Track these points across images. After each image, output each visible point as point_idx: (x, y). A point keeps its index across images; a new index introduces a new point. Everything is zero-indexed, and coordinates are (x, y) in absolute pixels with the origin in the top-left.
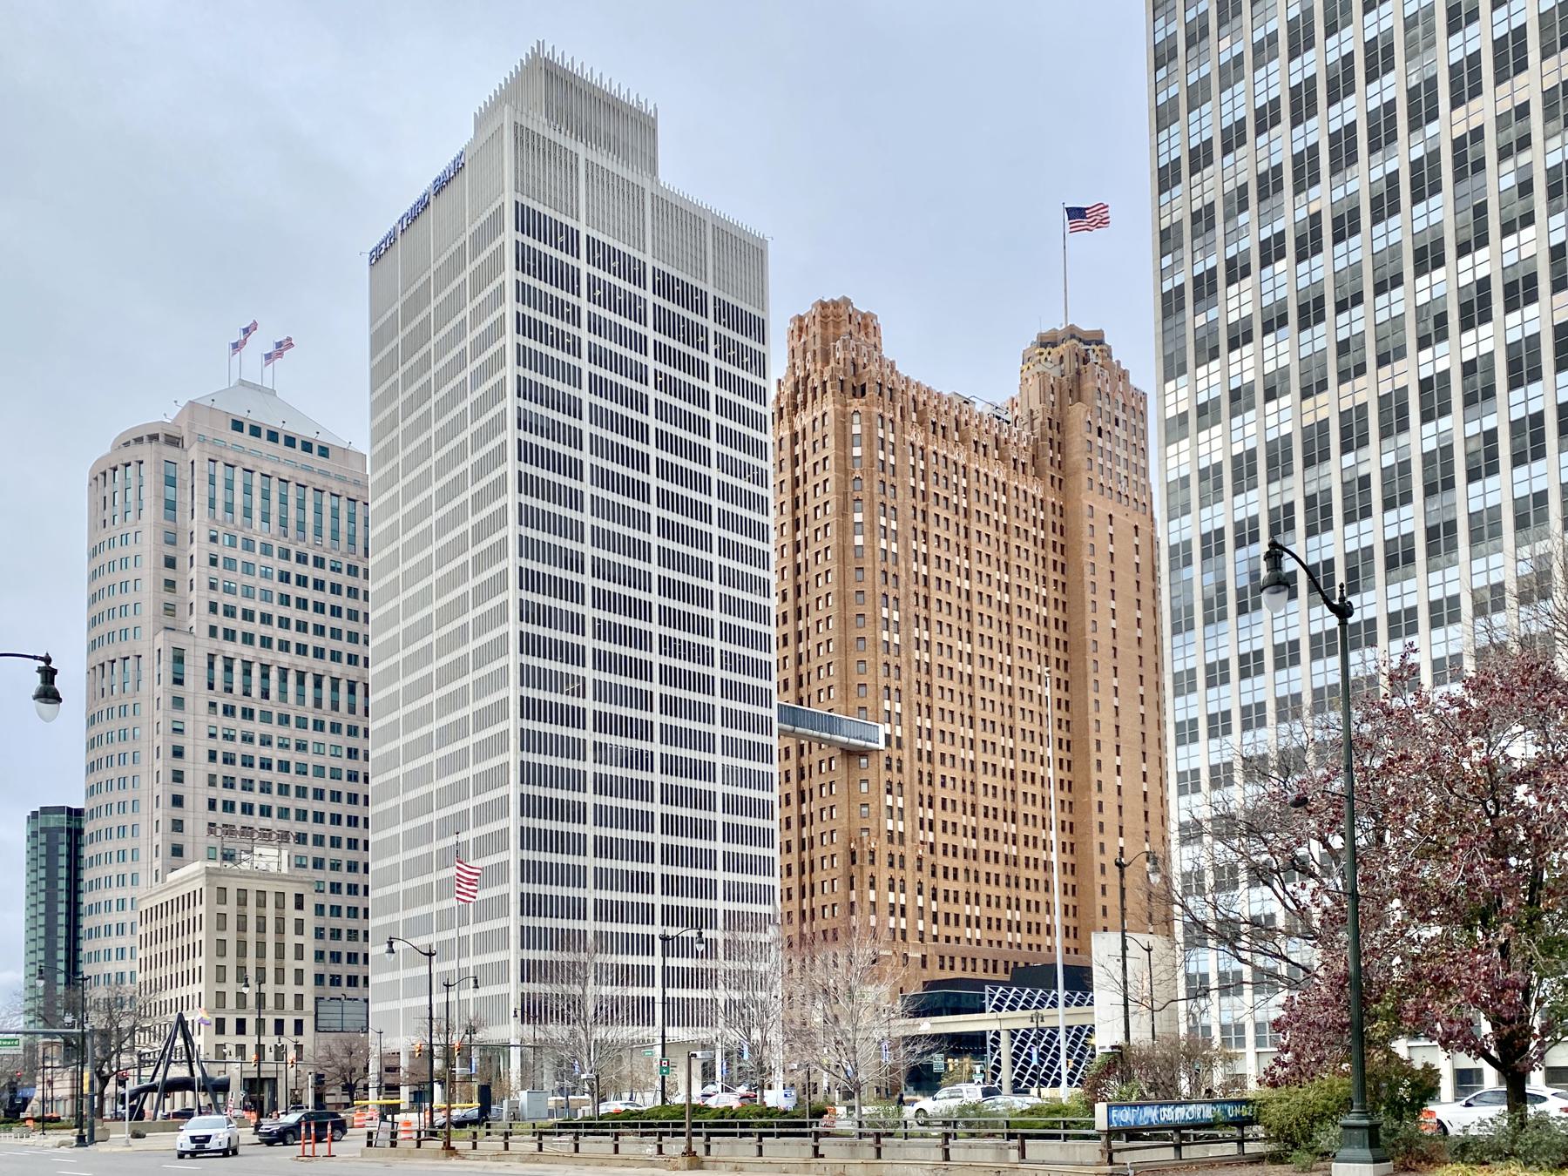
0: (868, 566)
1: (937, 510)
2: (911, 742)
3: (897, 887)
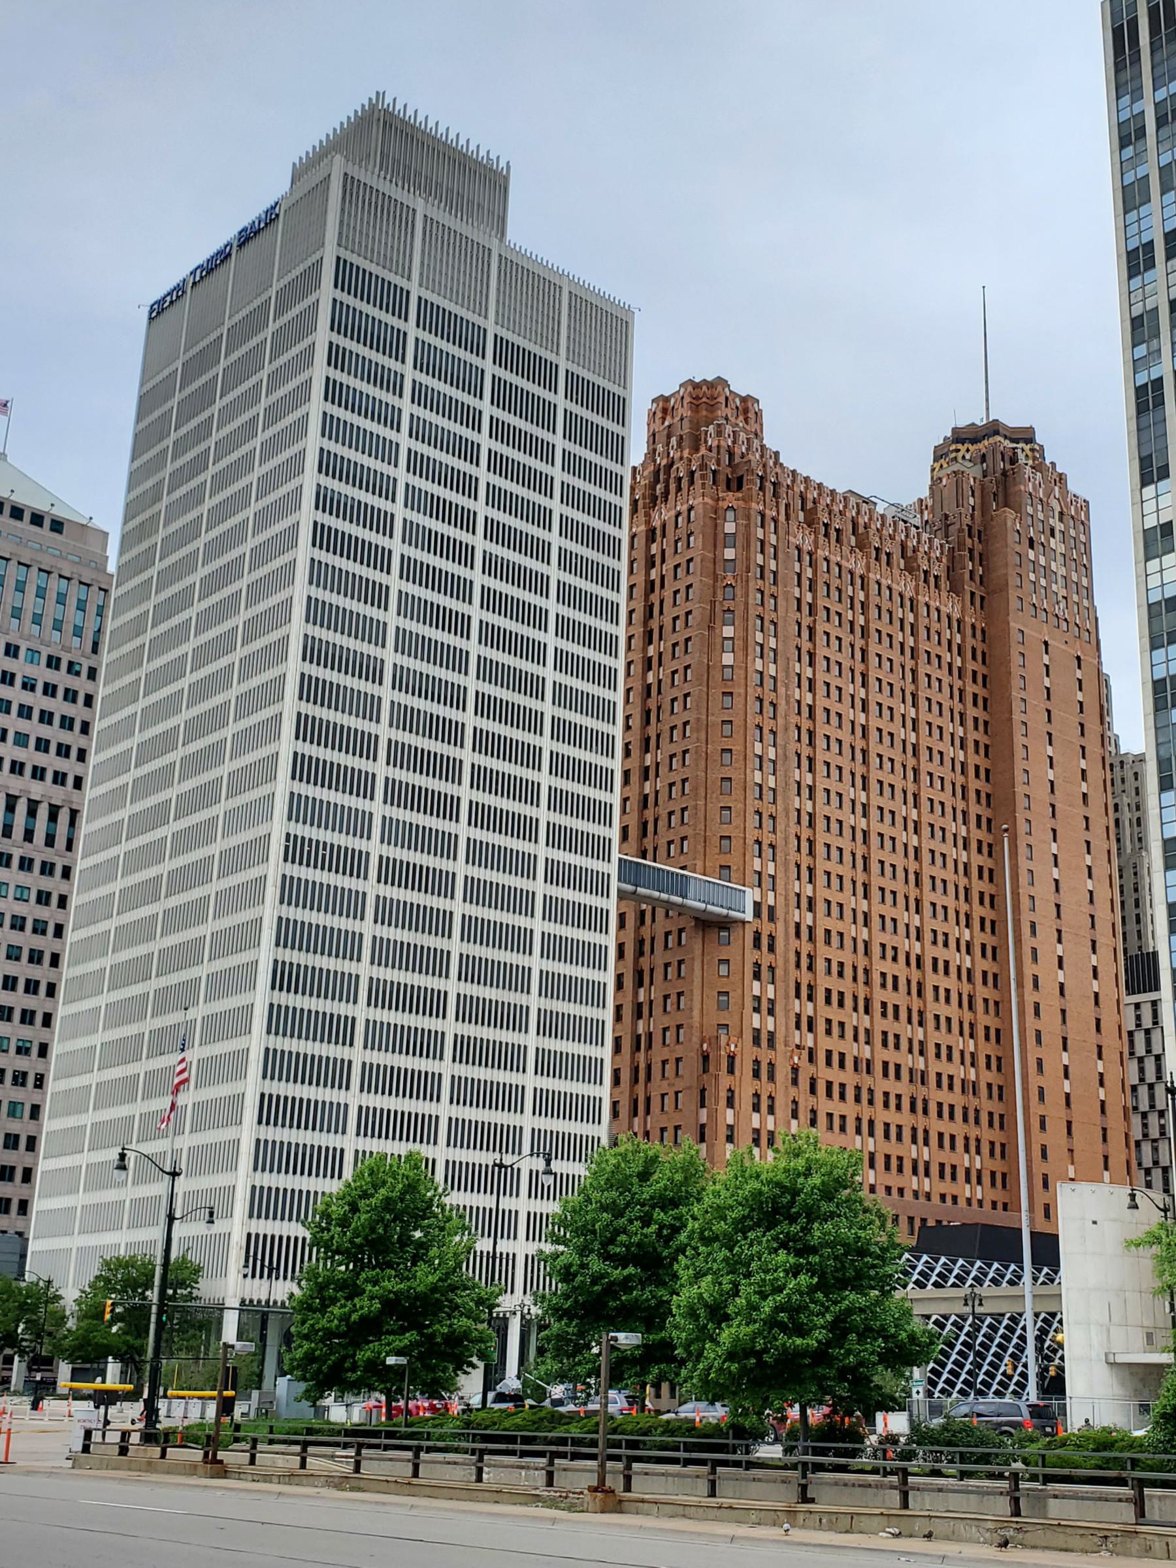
0: (738, 690)
1: (827, 627)
2: (787, 913)
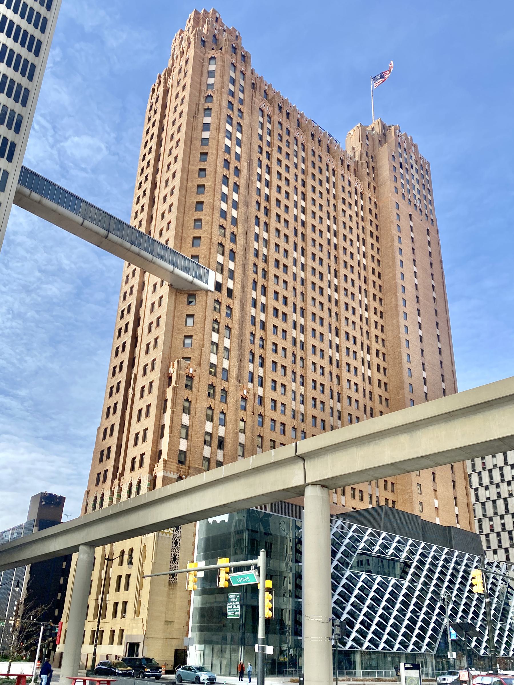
3: (216, 418)
